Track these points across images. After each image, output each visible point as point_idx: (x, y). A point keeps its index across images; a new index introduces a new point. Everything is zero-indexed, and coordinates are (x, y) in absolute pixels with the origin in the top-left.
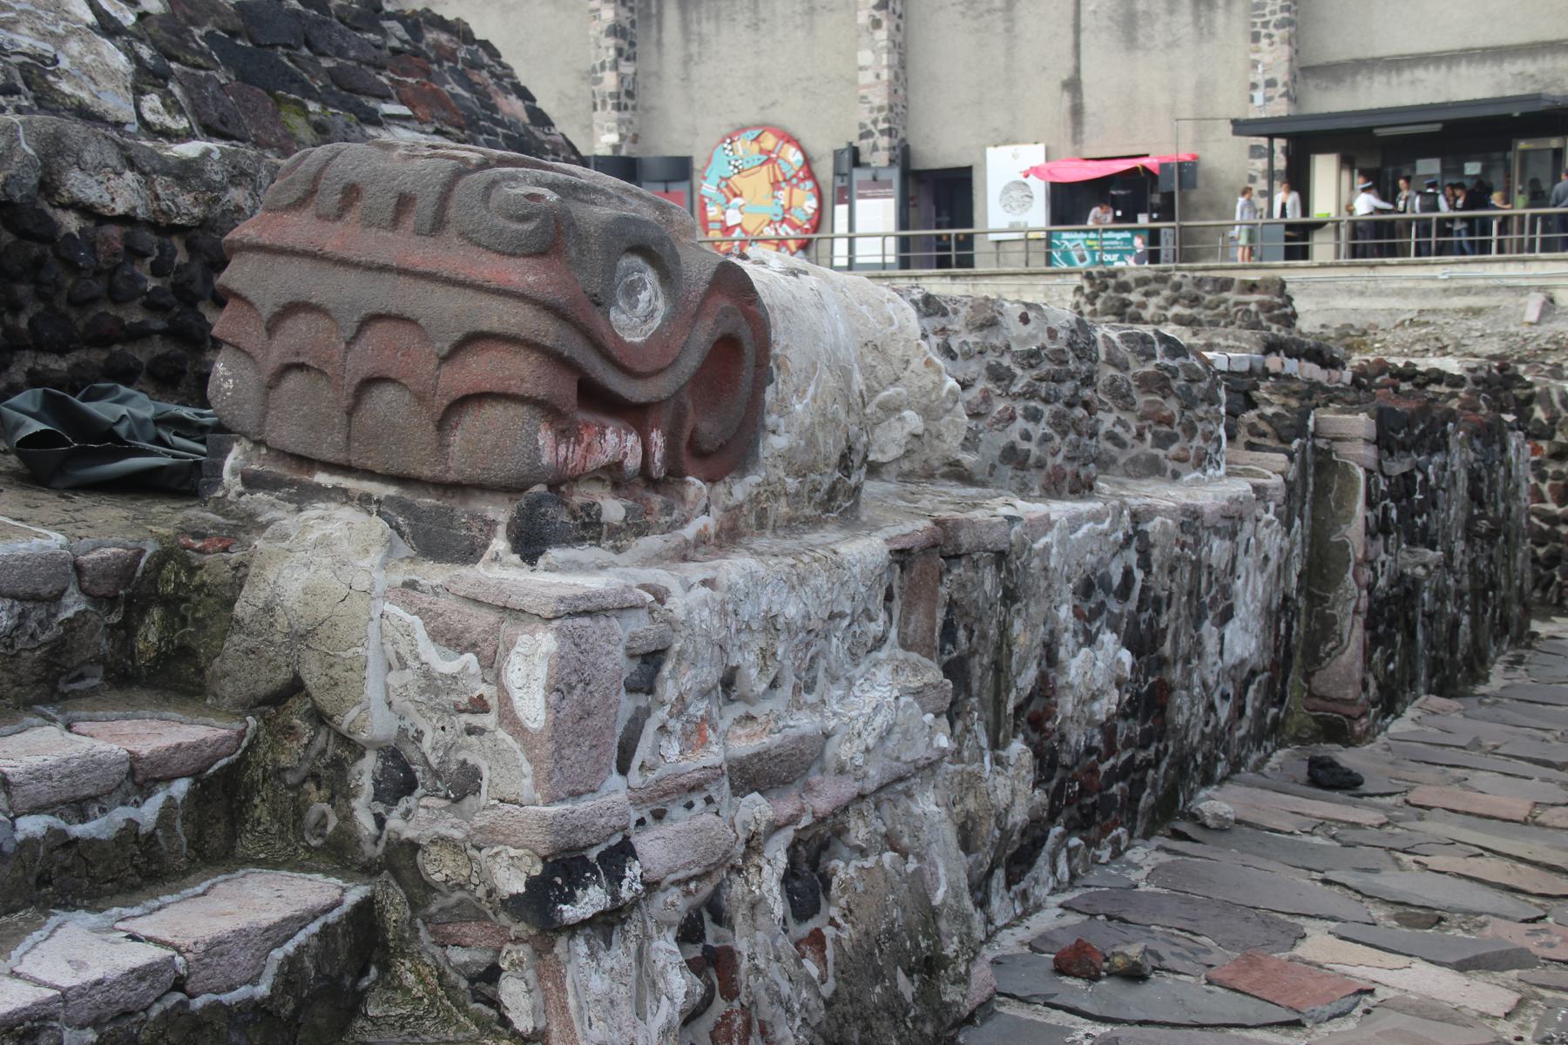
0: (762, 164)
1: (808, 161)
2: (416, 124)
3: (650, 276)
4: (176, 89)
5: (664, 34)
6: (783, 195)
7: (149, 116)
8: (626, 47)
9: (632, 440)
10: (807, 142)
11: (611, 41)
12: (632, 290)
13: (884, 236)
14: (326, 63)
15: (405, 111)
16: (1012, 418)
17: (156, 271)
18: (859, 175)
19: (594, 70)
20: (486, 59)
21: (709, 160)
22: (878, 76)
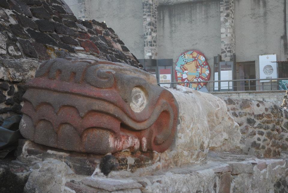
0: (193, 61)
1: (206, 60)
2: (85, 52)
3: (142, 94)
4: (18, 45)
5: (165, 24)
6: (199, 70)
7: (10, 52)
8: (154, 28)
9: (137, 141)
10: (206, 55)
11: (149, 27)
12: (137, 98)
13: (229, 81)
14: (60, 36)
15: (82, 48)
16: (255, 134)
17: (9, 94)
18: (221, 64)
19: (145, 35)
20: (110, 33)
21: (178, 60)
22: (227, 35)
